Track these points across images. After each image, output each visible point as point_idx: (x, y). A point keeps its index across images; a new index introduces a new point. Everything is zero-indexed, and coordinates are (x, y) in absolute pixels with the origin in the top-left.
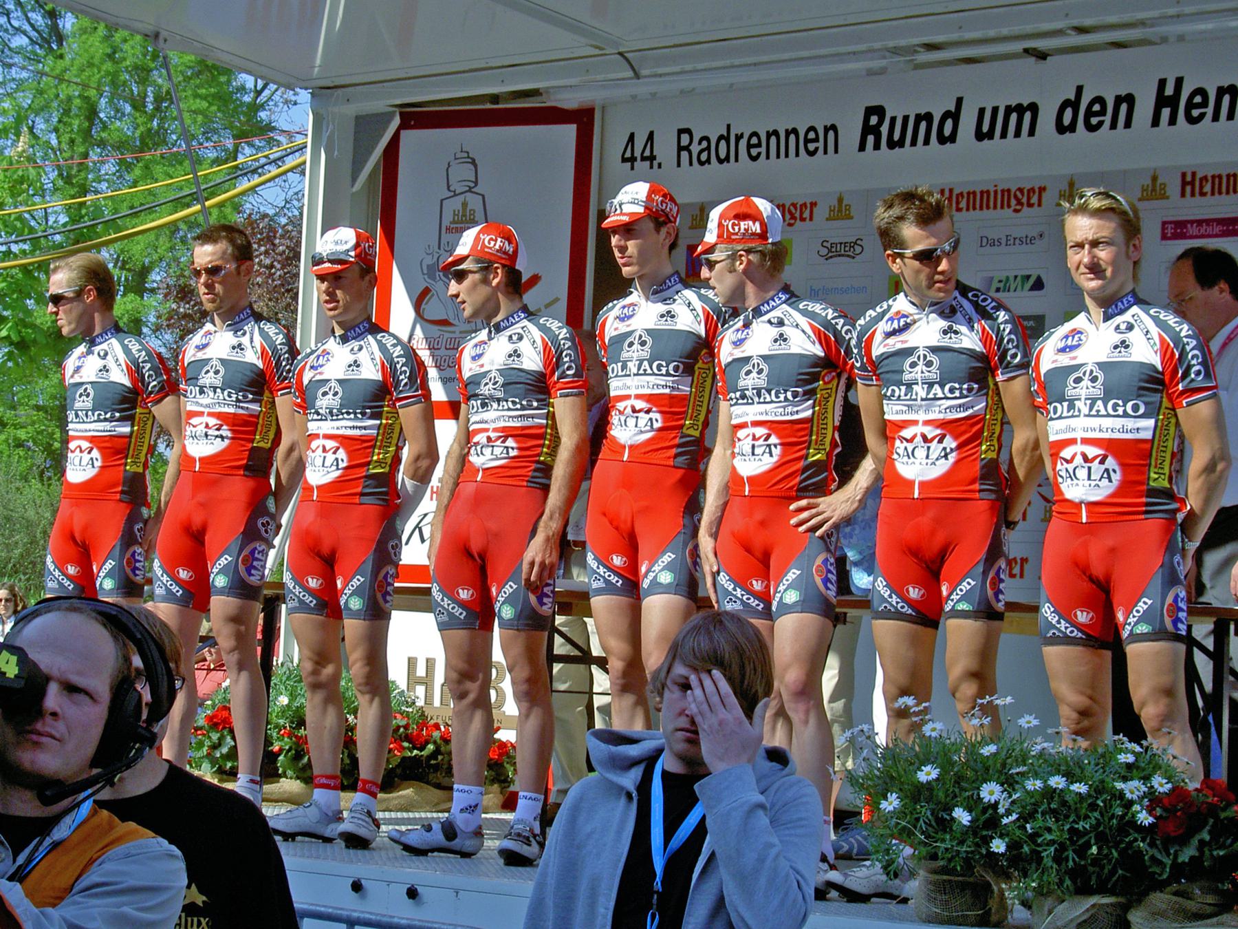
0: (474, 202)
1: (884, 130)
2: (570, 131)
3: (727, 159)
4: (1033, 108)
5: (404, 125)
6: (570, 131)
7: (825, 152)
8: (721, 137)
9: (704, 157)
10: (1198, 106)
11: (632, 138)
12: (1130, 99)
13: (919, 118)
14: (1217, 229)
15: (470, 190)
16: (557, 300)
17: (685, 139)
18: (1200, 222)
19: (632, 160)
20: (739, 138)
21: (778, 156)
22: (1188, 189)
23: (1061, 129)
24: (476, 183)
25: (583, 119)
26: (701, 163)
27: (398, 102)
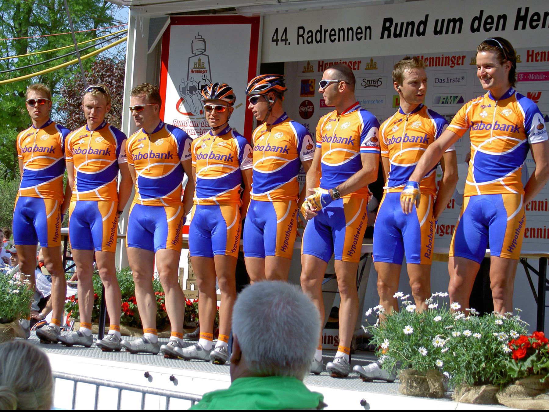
0: (204, 59)
1: (392, 29)
2: (248, 27)
4: (461, 20)
5: (172, 23)
6: (249, 27)
7: (365, 39)
8: (318, 31)
9: (310, 40)
10: (535, 21)
11: (277, 30)
12: (504, 17)
13: (408, 24)
14: (543, 77)
15: (202, 54)
16: (241, 104)
17: (301, 32)
18: (535, 74)
19: (277, 41)
20: (326, 31)
21: (344, 40)
22: (530, 58)
23: (473, 30)
24: (205, 50)
25: (255, 22)
26: (308, 43)
27: (170, 12)
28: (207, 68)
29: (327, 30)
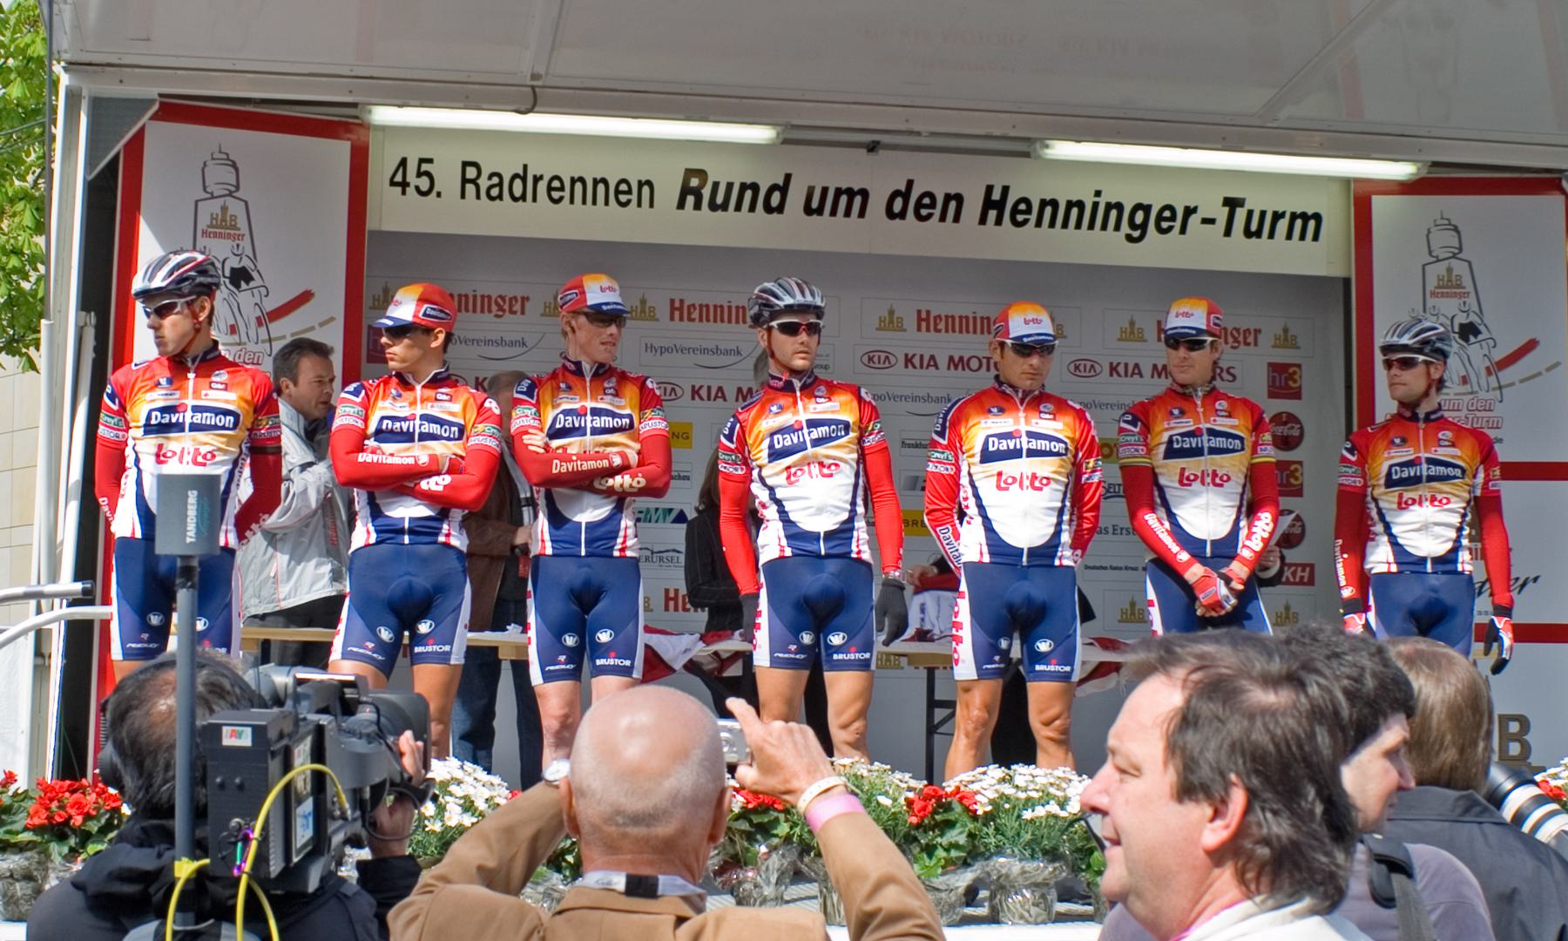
0: (235, 208)
1: (706, 192)
2: (340, 150)
3: (523, 197)
4: (864, 194)
6: (340, 150)
7: (639, 205)
9: (495, 192)
12: (959, 198)
13: (744, 187)
15: (230, 194)
20: (537, 179)
21: (584, 202)
23: (891, 214)
24: (238, 188)
26: (491, 198)
28: (244, 230)
29: (541, 177)
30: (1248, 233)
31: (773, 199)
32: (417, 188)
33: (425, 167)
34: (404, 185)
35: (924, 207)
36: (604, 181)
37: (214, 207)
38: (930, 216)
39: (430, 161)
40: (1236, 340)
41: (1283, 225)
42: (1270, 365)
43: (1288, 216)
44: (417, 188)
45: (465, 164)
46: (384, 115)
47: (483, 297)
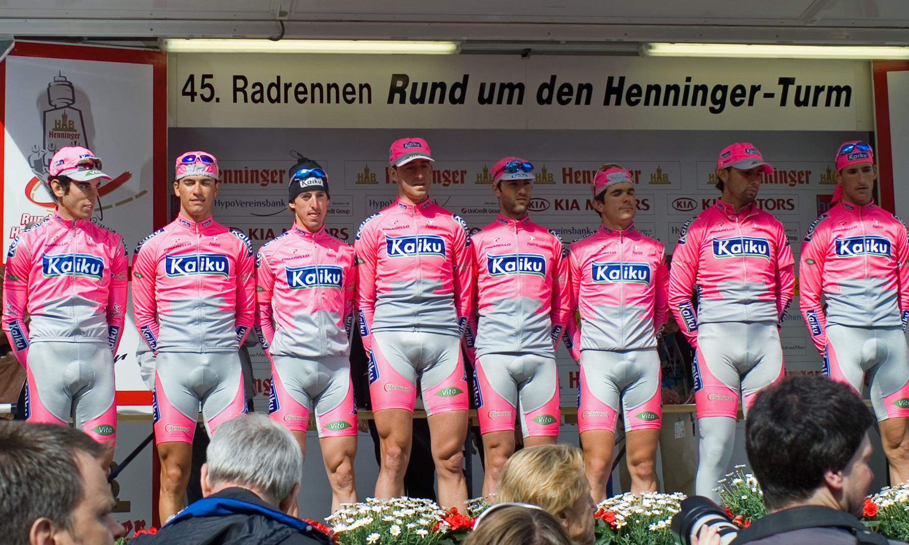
0: (72, 115)
1: (408, 90)
2: (147, 70)
3: (278, 100)
4: (521, 87)
6: (147, 70)
8: (272, 85)
9: (258, 97)
10: (635, 95)
12: (589, 87)
13: (435, 86)
15: (69, 106)
17: (240, 84)
20: (287, 86)
21: (322, 101)
23: (541, 101)
24: (74, 101)
29: (290, 85)
30: (798, 103)
31: (455, 94)
32: (202, 96)
33: (207, 81)
34: (193, 94)
35: (565, 94)
36: (335, 86)
37: (58, 115)
38: (569, 101)
39: (211, 76)
40: (793, 180)
41: (823, 96)
42: (818, 196)
43: (826, 89)
44: (202, 96)
45: (236, 78)
46: (177, 45)
47: (252, 171)
